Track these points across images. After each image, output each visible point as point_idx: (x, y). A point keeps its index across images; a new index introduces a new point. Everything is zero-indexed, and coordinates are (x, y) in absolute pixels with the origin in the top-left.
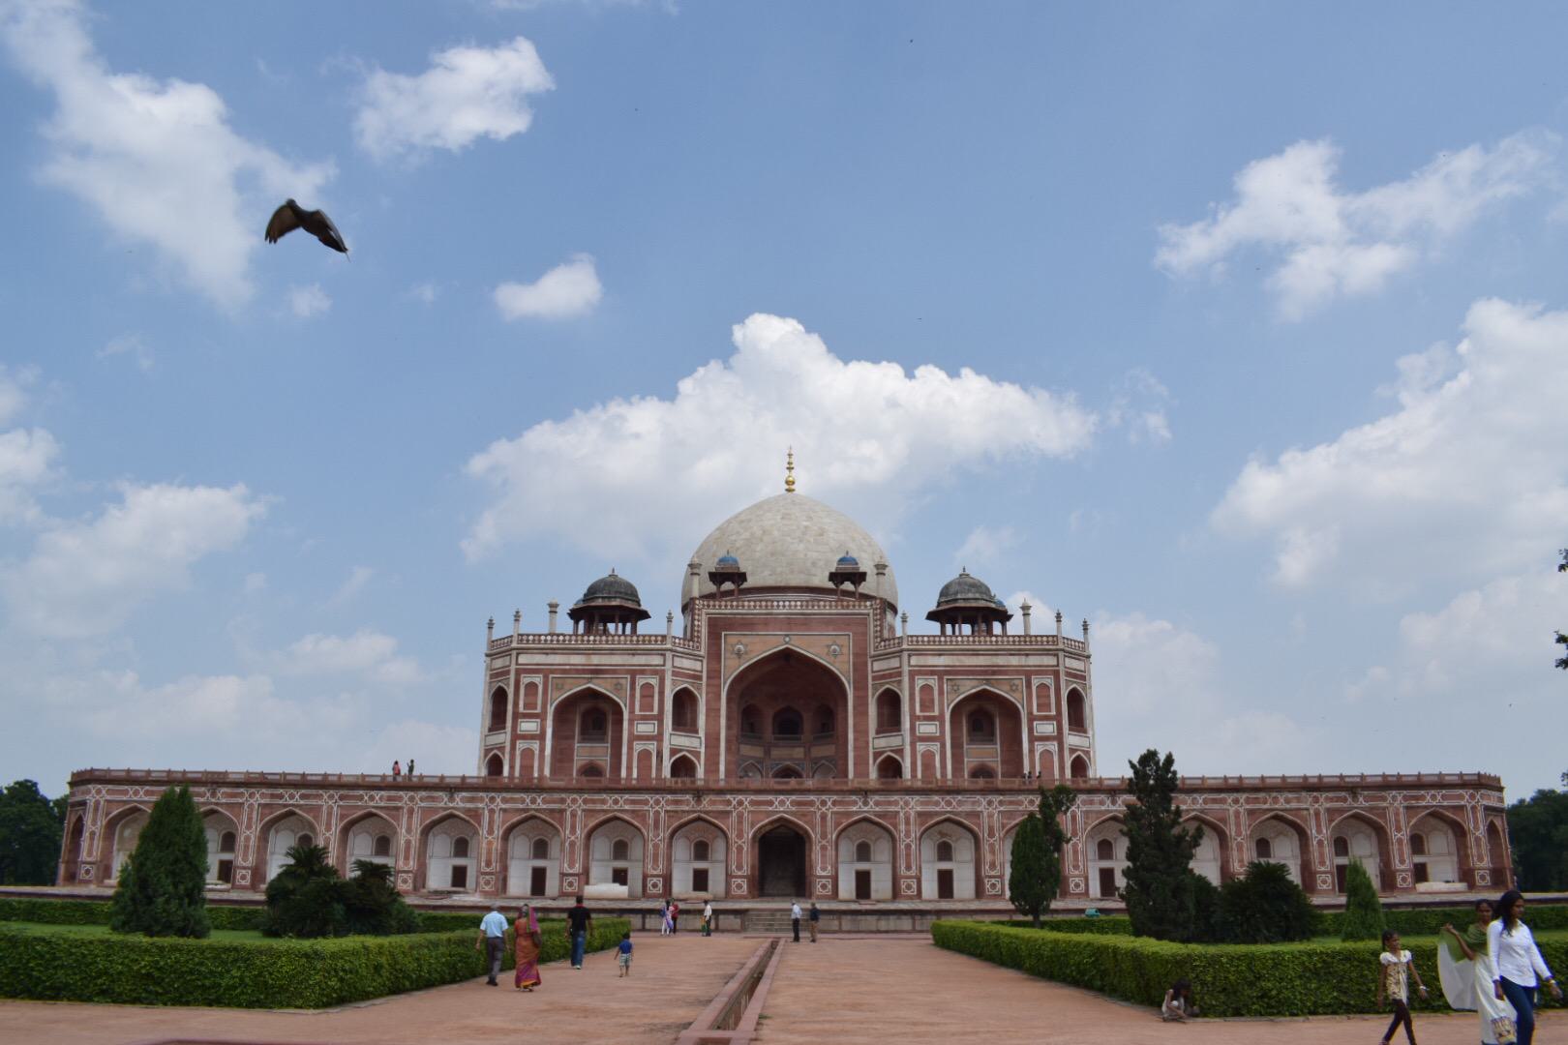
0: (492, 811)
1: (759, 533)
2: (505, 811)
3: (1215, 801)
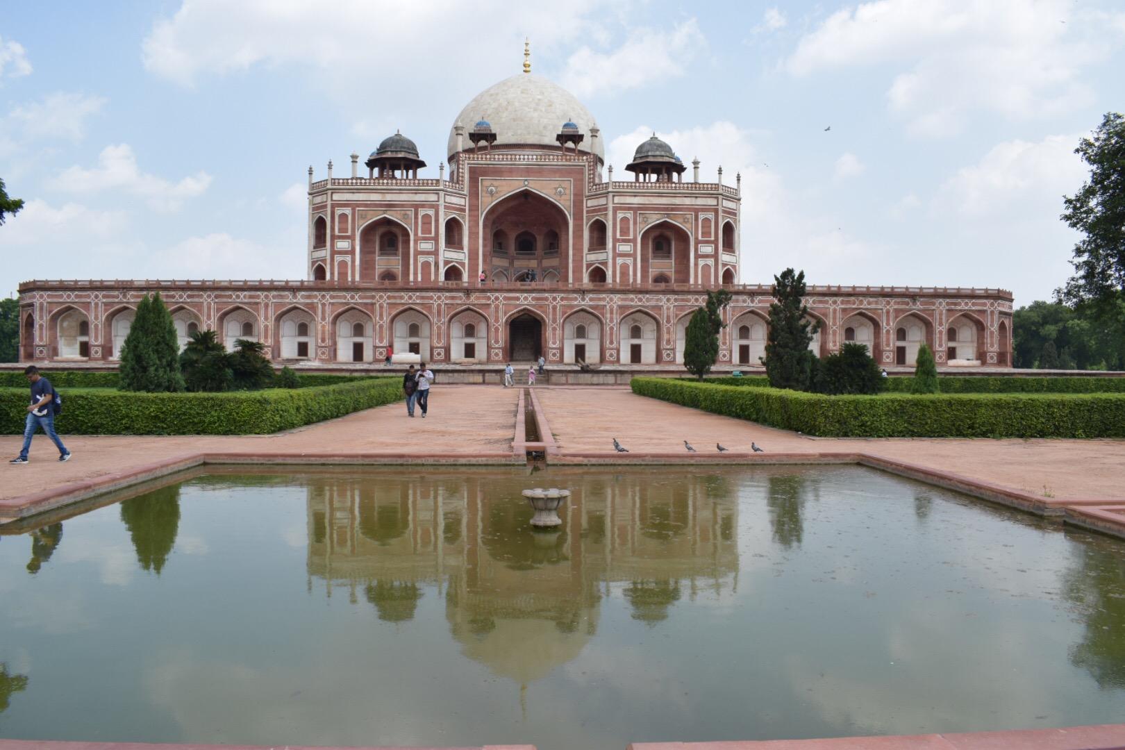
0: (324, 305)
1: (505, 104)
2: (333, 304)
3: (821, 302)
